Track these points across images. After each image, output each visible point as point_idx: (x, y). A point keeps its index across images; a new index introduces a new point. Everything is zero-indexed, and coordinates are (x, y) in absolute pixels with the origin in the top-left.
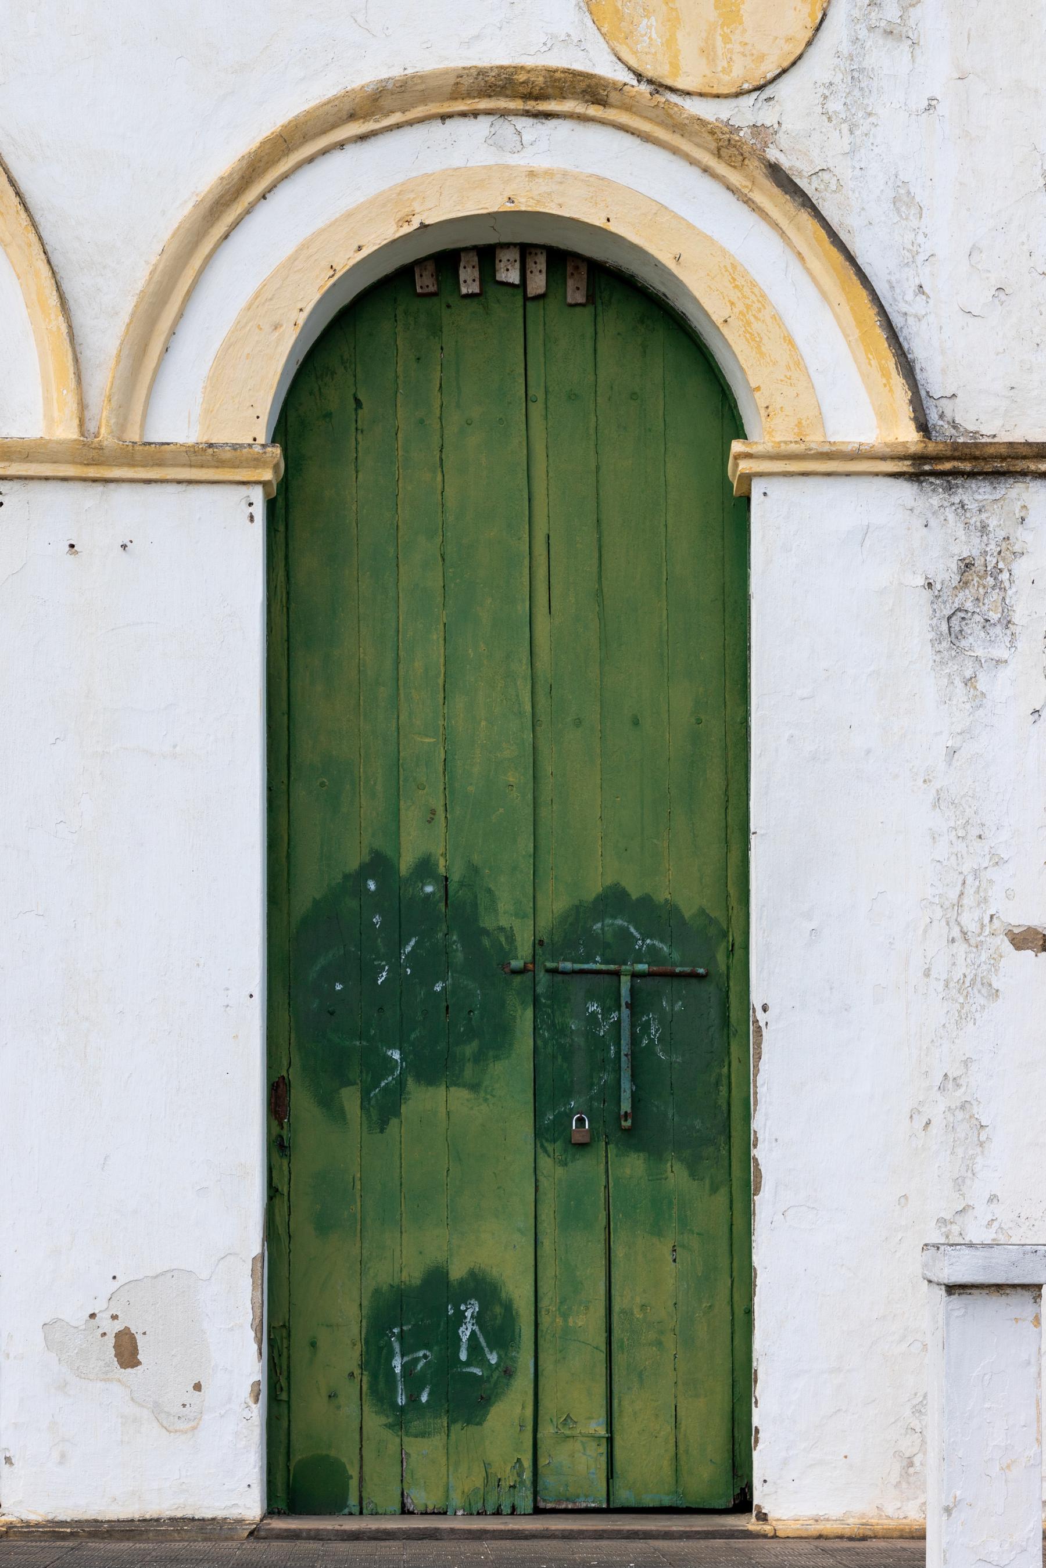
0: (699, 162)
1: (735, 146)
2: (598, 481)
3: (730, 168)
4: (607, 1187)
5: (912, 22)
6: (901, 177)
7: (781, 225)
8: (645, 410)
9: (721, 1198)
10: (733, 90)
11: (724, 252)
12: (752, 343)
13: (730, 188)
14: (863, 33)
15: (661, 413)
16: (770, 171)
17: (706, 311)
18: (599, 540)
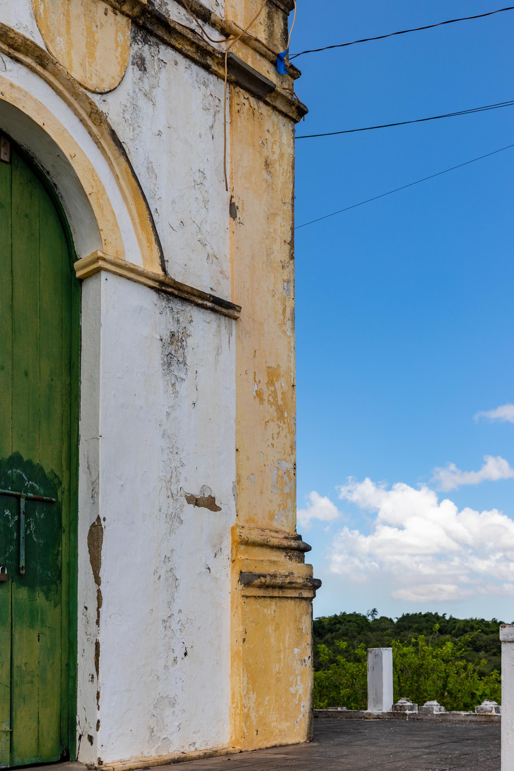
0: (81, 115)
1: (99, 115)
2: (12, 252)
3: (93, 124)
4: (12, 603)
5: (153, 94)
6: (150, 159)
7: (111, 159)
8: (31, 224)
9: (58, 610)
10: (93, 89)
11: (90, 163)
12: (100, 208)
13: (90, 133)
14: (137, 90)
15: (38, 228)
16: (112, 132)
17: (82, 186)
18: (12, 280)
